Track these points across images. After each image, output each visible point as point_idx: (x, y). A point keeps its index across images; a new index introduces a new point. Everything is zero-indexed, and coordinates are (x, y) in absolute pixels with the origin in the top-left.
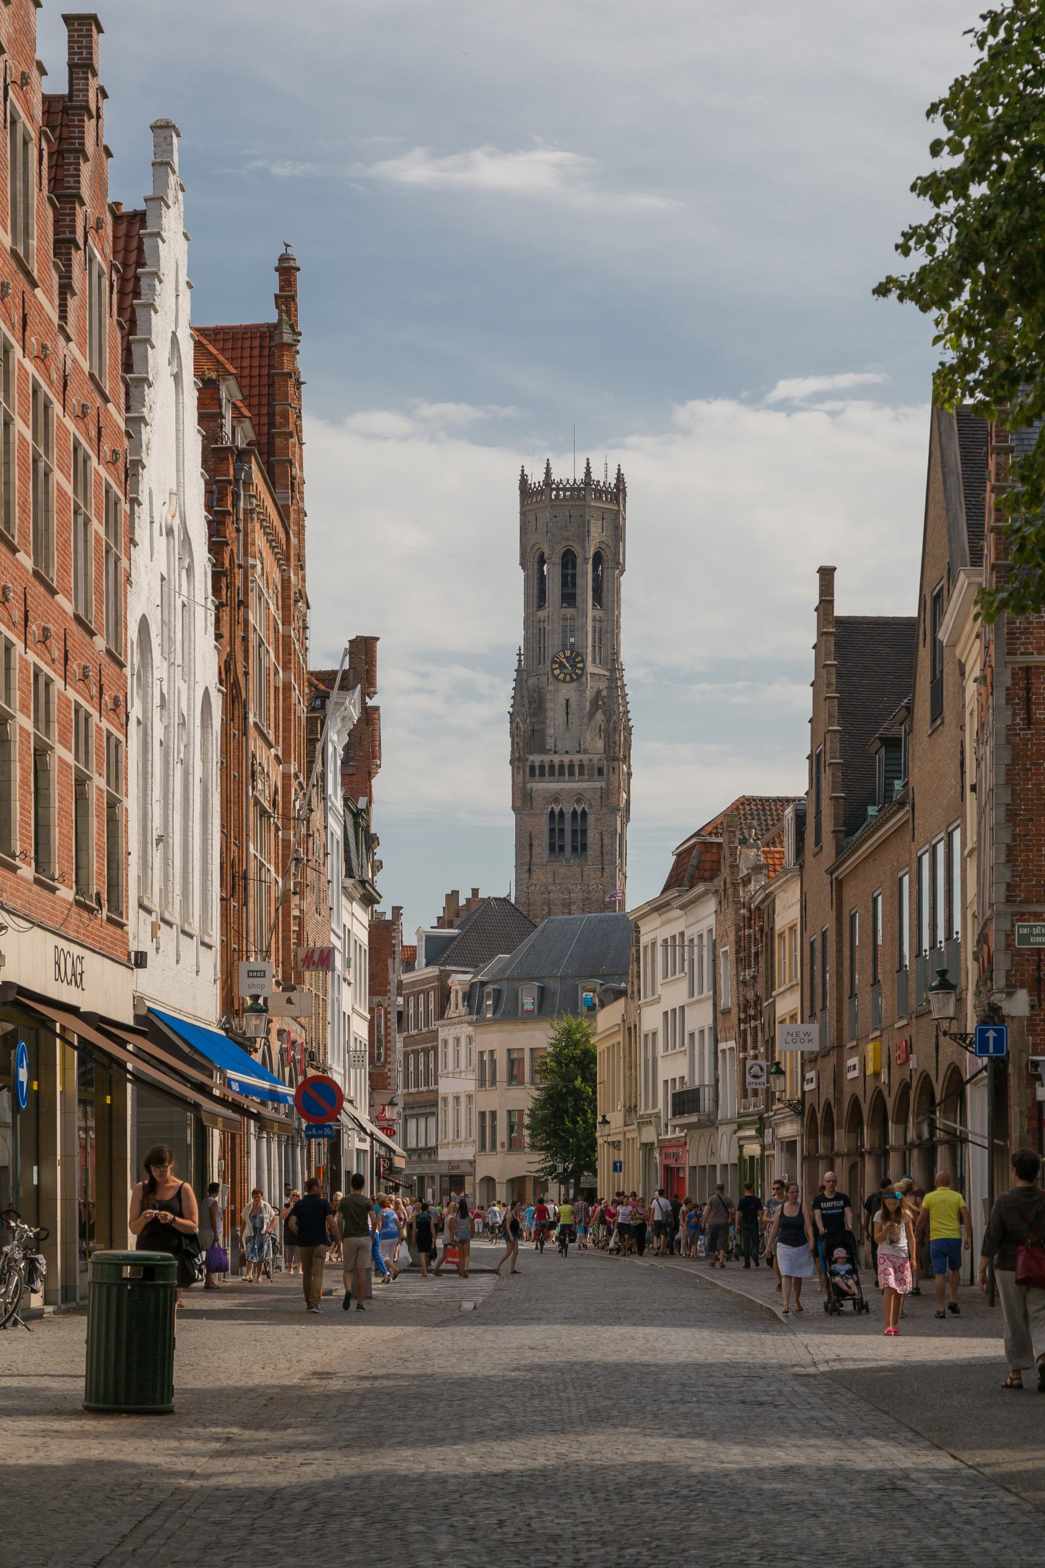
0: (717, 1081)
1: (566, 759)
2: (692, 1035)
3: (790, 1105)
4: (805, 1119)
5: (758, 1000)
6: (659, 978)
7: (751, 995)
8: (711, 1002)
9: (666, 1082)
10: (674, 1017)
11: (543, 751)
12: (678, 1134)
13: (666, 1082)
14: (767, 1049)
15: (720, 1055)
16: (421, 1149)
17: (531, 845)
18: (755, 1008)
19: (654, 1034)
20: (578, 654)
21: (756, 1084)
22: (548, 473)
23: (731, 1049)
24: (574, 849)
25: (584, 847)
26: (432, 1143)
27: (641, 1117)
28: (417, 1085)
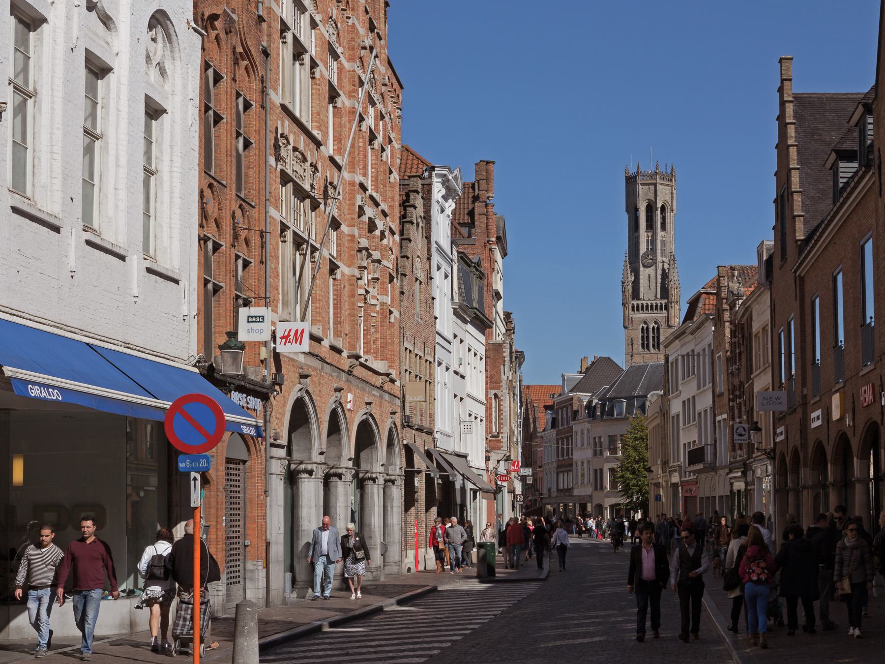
0: (715, 441)
1: (649, 303)
2: (700, 414)
3: (766, 453)
4: (777, 462)
5: (742, 384)
6: (680, 381)
7: (736, 382)
8: (711, 390)
9: (685, 445)
10: (690, 404)
11: (639, 299)
12: (692, 477)
14: (748, 417)
15: (717, 424)
16: (565, 490)
17: (632, 344)
18: (740, 390)
19: (678, 416)
21: (741, 440)
23: (724, 419)
24: (654, 346)
26: (571, 486)
27: (671, 467)
28: (563, 456)
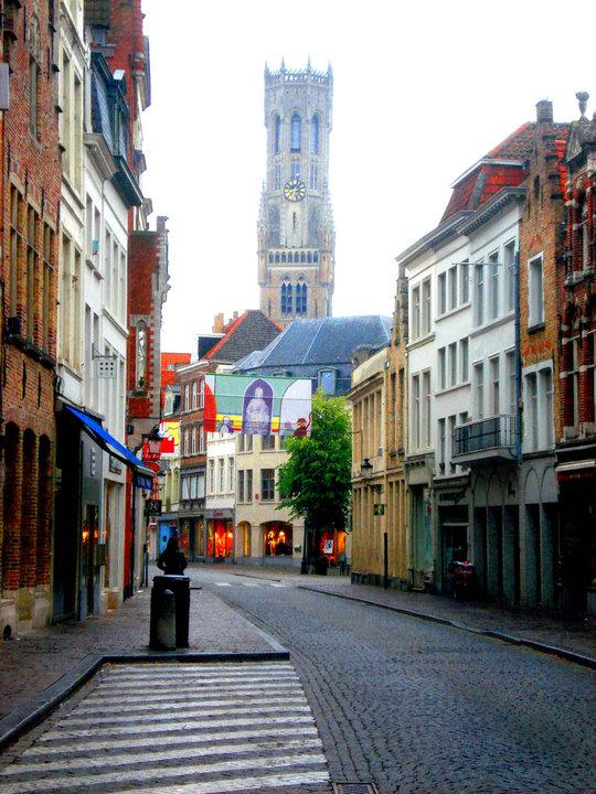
0: (520, 410)
1: (293, 251)
2: (479, 368)
6: (435, 315)
8: (514, 322)
9: (442, 421)
13: (442, 421)
15: (524, 381)
16: (192, 500)
19: (427, 374)
20: (302, 183)
22: (283, 65)
23: (546, 372)
25: (305, 309)
26: (201, 496)
28: (190, 451)
